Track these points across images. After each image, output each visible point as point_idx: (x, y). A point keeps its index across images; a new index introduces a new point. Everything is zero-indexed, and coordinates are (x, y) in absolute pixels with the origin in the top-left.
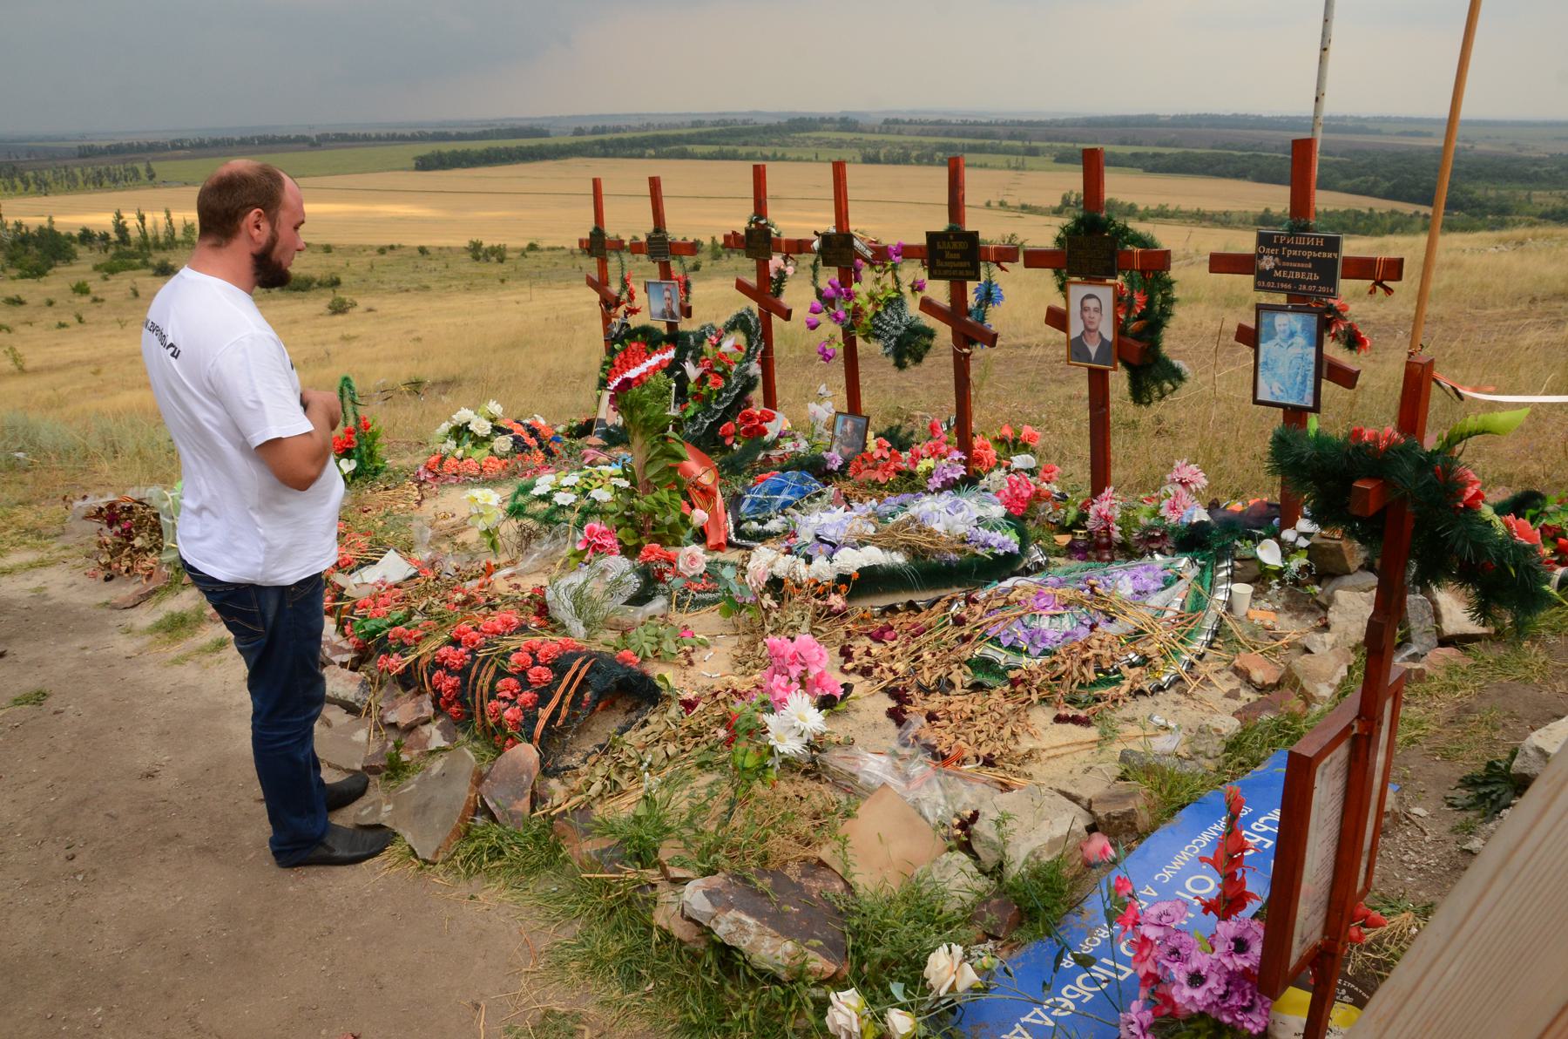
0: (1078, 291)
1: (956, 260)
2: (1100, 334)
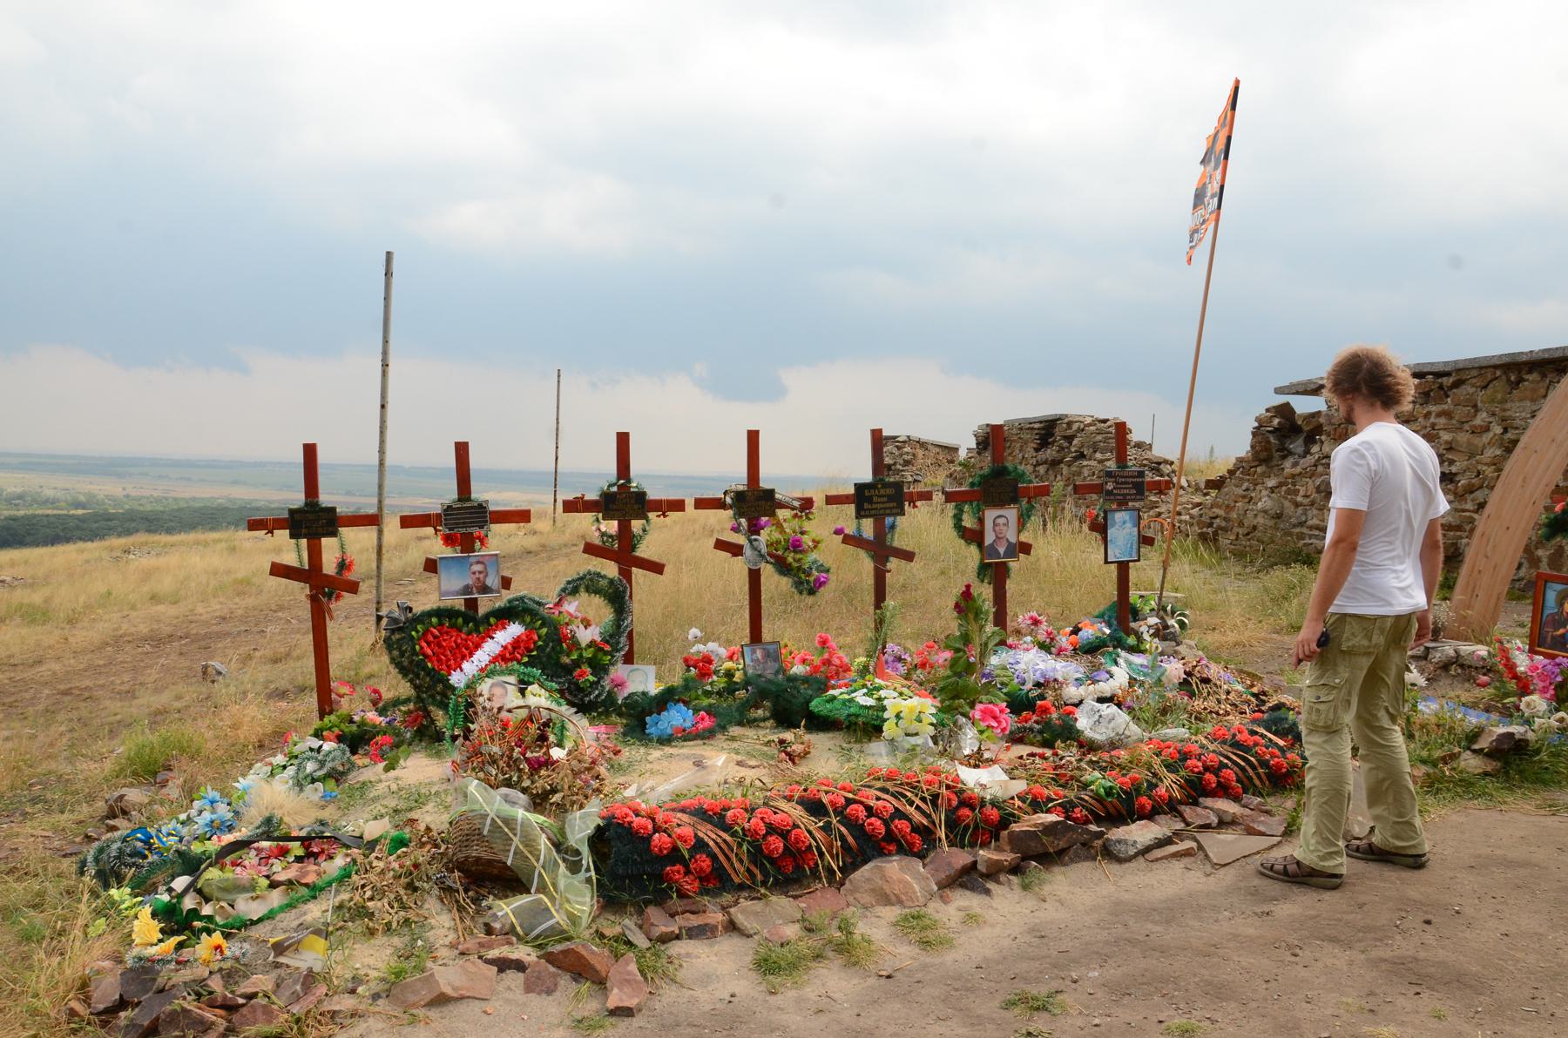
0: (990, 515)
1: (883, 503)
2: (1007, 540)
